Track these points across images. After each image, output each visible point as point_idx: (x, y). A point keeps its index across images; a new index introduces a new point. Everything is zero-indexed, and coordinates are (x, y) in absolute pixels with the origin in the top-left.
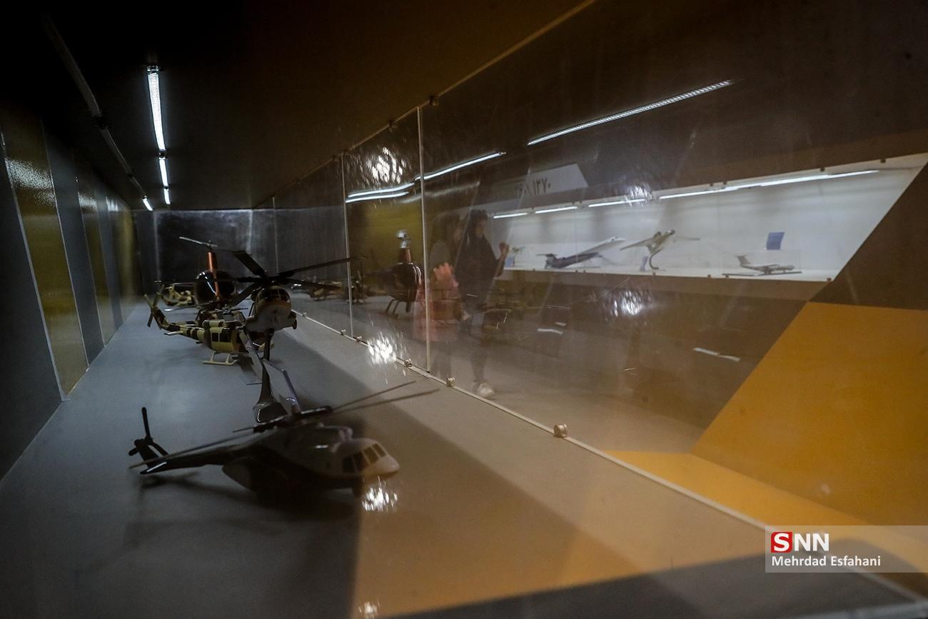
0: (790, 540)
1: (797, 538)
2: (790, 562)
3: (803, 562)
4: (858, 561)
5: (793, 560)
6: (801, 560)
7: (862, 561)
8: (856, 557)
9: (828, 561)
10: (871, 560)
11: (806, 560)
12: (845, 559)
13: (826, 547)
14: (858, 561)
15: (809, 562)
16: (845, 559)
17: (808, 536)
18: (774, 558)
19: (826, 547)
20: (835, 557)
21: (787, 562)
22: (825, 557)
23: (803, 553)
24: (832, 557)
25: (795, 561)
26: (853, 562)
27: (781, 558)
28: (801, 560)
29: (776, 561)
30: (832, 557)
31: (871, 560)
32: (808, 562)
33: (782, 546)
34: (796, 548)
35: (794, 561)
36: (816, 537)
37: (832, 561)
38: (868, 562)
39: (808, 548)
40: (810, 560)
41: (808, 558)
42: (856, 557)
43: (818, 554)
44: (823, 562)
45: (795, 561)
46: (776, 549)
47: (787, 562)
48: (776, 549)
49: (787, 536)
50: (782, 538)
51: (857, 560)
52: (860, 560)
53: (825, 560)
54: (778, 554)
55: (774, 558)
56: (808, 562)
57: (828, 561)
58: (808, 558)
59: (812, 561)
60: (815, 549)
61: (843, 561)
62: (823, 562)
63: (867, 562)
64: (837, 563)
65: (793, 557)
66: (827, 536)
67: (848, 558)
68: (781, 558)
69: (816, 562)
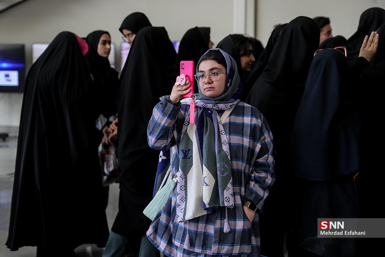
0: (328, 224)
1: (331, 223)
2: (328, 233)
3: (333, 233)
4: (356, 233)
5: (329, 233)
6: (332, 233)
7: (358, 233)
8: (355, 231)
9: (344, 233)
10: (362, 233)
11: (334, 232)
12: (351, 232)
13: (343, 227)
14: (356, 233)
15: (335, 233)
16: (351, 232)
17: (335, 222)
18: (321, 232)
19: (343, 227)
20: (347, 231)
21: (326, 233)
22: (342, 231)
23: (333, 230)
24: (345, 231)
25: (330, 233)
26: (354, 233)
27: (324, 232)
28: (332, 233)
29: (322, 233)
30: (345, 231)
31: (362, 233)
32: (335, 233)
33: (324, 227)
34: (330, 228)
35: (330, 233)
36: (339, 223)
37: (345, 233)
38: (360, 233)
39: (335, 227)
40: (336, 233)
41: (335, 232)
42: (355, 231)
43: (340, 230)
44: (341, 233)
45: (330, 233)
46: (322, 228)
47: (326, 233)
48: (322, 228)
49: (326, 222)
50: (324, 223)
51: (355, 232)
52: (357, 232)
53: (342, 232)
54: (323, 230)
55: (321, 232)
56: (335, 233)
57: (344, 233)
58: (335, 232)
59: (337, 233)
60: (338, 228)
61: (350, 233)
62: (341, 233)
63: (360, 234)
64: (347, 234)
65: (329, 231)
66: (343, 223)
67: (352, 232)
68: (324, 232)
69: (339, 234)
